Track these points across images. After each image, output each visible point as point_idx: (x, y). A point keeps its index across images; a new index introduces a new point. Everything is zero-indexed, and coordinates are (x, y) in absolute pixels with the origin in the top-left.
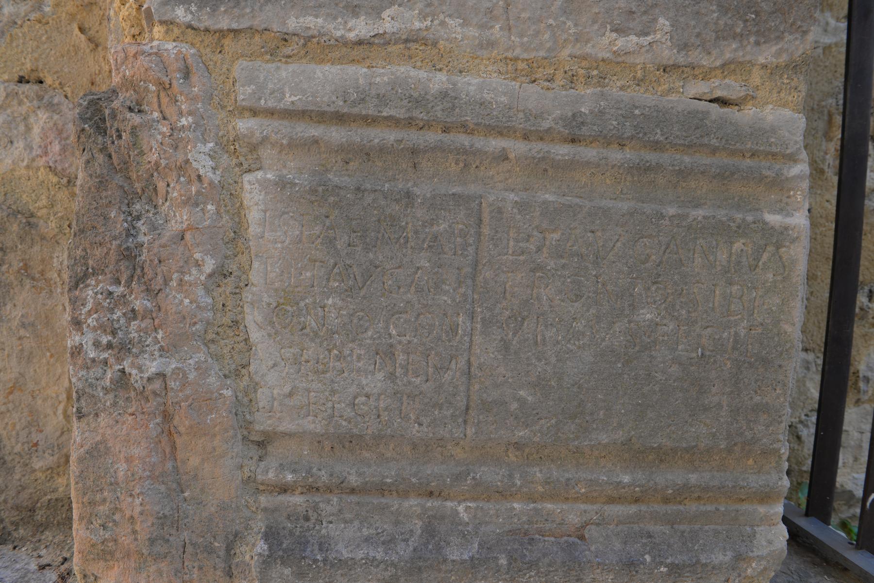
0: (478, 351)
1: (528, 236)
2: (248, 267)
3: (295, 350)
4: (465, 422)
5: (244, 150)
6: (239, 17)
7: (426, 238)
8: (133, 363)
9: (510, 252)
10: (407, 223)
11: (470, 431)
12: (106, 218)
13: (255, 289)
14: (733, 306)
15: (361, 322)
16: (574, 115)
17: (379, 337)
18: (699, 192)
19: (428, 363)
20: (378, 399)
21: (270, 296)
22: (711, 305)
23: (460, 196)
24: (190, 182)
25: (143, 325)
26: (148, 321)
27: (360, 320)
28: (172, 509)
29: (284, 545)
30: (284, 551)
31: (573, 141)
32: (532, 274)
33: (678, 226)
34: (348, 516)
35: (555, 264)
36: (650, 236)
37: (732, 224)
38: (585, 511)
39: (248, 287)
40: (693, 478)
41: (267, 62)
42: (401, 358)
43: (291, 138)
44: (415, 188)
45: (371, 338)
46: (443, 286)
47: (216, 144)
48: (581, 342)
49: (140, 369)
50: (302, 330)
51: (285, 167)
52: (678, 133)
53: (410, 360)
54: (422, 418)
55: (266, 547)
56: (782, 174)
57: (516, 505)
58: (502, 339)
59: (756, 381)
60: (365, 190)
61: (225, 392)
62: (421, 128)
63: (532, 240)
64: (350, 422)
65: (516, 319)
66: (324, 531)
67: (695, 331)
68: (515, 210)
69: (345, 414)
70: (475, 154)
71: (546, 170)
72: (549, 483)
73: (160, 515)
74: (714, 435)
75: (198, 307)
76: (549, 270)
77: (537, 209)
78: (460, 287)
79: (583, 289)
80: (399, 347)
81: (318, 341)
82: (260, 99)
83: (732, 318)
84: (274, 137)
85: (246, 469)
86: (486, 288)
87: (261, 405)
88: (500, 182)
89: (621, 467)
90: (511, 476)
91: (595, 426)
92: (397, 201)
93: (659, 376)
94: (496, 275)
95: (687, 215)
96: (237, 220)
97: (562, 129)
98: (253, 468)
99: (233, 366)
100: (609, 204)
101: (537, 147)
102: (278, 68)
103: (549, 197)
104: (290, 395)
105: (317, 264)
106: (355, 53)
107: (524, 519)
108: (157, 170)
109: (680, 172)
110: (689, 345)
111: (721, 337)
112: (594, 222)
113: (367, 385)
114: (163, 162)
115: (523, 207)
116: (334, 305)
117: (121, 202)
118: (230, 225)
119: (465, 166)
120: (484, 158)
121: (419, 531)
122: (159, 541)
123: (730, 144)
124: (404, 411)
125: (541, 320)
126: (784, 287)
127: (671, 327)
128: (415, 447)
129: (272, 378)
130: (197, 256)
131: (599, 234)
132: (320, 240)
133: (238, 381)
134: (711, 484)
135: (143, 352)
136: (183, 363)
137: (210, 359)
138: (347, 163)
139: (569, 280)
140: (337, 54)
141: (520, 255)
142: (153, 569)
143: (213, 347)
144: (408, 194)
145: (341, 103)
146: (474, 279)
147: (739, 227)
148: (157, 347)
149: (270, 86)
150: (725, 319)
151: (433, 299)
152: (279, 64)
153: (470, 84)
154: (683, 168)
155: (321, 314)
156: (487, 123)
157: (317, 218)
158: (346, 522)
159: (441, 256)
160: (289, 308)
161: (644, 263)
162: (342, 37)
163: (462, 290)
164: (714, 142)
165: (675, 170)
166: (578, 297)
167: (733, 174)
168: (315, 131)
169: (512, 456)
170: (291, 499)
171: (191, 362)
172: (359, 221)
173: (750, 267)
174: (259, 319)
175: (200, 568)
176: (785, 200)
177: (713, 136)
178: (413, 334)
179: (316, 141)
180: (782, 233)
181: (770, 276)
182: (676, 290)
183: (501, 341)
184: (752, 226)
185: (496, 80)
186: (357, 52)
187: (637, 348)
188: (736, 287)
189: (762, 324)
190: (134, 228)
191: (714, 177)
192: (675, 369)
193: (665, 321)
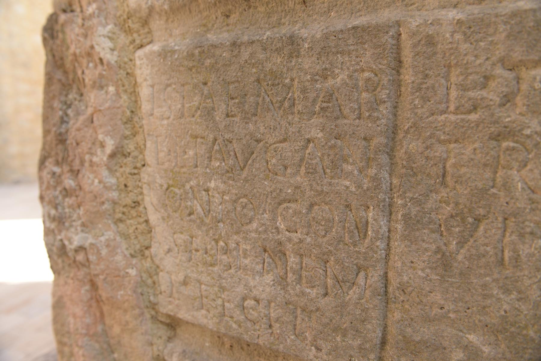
0: (399, 264)
2: (143, 147)
7: (318, 96)
9: (452, 108)
10: (292, 80)
13: (149, 169)
15: (245, 211)
17: (265, 231)
19: (326, 271)
20: (268, 306)
21: (161, 177)
24: (96, 66)
27: (244, 207)
32: (494, 143)
39: (144, 168)
42: (293, 260)
44: (303, 31)
45: (256, 231)
46: (345, 166)
47: (115, 25)
49: (69, 240)
50: (190, 214)
51: (171, 35)
53: (304, 265)
58: (438, 250)
60: (242, 43)
61: (130, 271)
63: (492, 84)
64: (240, 326)
65: (463, 219)
68: (458, 36)
69: (235, 315)
75: (105, 187)
76: (528, 137)
77: (501, 27)
80: (289, 246)
81: (204, 228)
85: (155, 348)
86: (412, 168)
87: (163, 288)
92: (278, 51)
94: (427, 148)
96: (133, 99)
98: (161, 348)
99: (138, 247)
104: (185, 283)
105: (199, 140)
108: (76, 60)
113: (255, 287)
114: (78, 51)
116: (216, 189)
117: (61, 94)
118: (127, 104)
124: (298, 327)
125: (511, 223)
129: (168, 263)
130: (100, 137)
132: (199, 112)
133: (143, 261)
135: (71, 226)
136: (96, 239)
137: (118, 238)
138: (228, 16)
141: (469, 112)
143: (121, 226)
148: (79, 222)
151: (330, 184)
155: (205, 198)
157: (195, 86)
159: (339, 122)
160: (176, 190)
163: (372, 172)
171: (102, 239)
172: (236, 84)
174: (155, 201)
178: (305, 231)
183: (436, 252)
190: (67, 115)
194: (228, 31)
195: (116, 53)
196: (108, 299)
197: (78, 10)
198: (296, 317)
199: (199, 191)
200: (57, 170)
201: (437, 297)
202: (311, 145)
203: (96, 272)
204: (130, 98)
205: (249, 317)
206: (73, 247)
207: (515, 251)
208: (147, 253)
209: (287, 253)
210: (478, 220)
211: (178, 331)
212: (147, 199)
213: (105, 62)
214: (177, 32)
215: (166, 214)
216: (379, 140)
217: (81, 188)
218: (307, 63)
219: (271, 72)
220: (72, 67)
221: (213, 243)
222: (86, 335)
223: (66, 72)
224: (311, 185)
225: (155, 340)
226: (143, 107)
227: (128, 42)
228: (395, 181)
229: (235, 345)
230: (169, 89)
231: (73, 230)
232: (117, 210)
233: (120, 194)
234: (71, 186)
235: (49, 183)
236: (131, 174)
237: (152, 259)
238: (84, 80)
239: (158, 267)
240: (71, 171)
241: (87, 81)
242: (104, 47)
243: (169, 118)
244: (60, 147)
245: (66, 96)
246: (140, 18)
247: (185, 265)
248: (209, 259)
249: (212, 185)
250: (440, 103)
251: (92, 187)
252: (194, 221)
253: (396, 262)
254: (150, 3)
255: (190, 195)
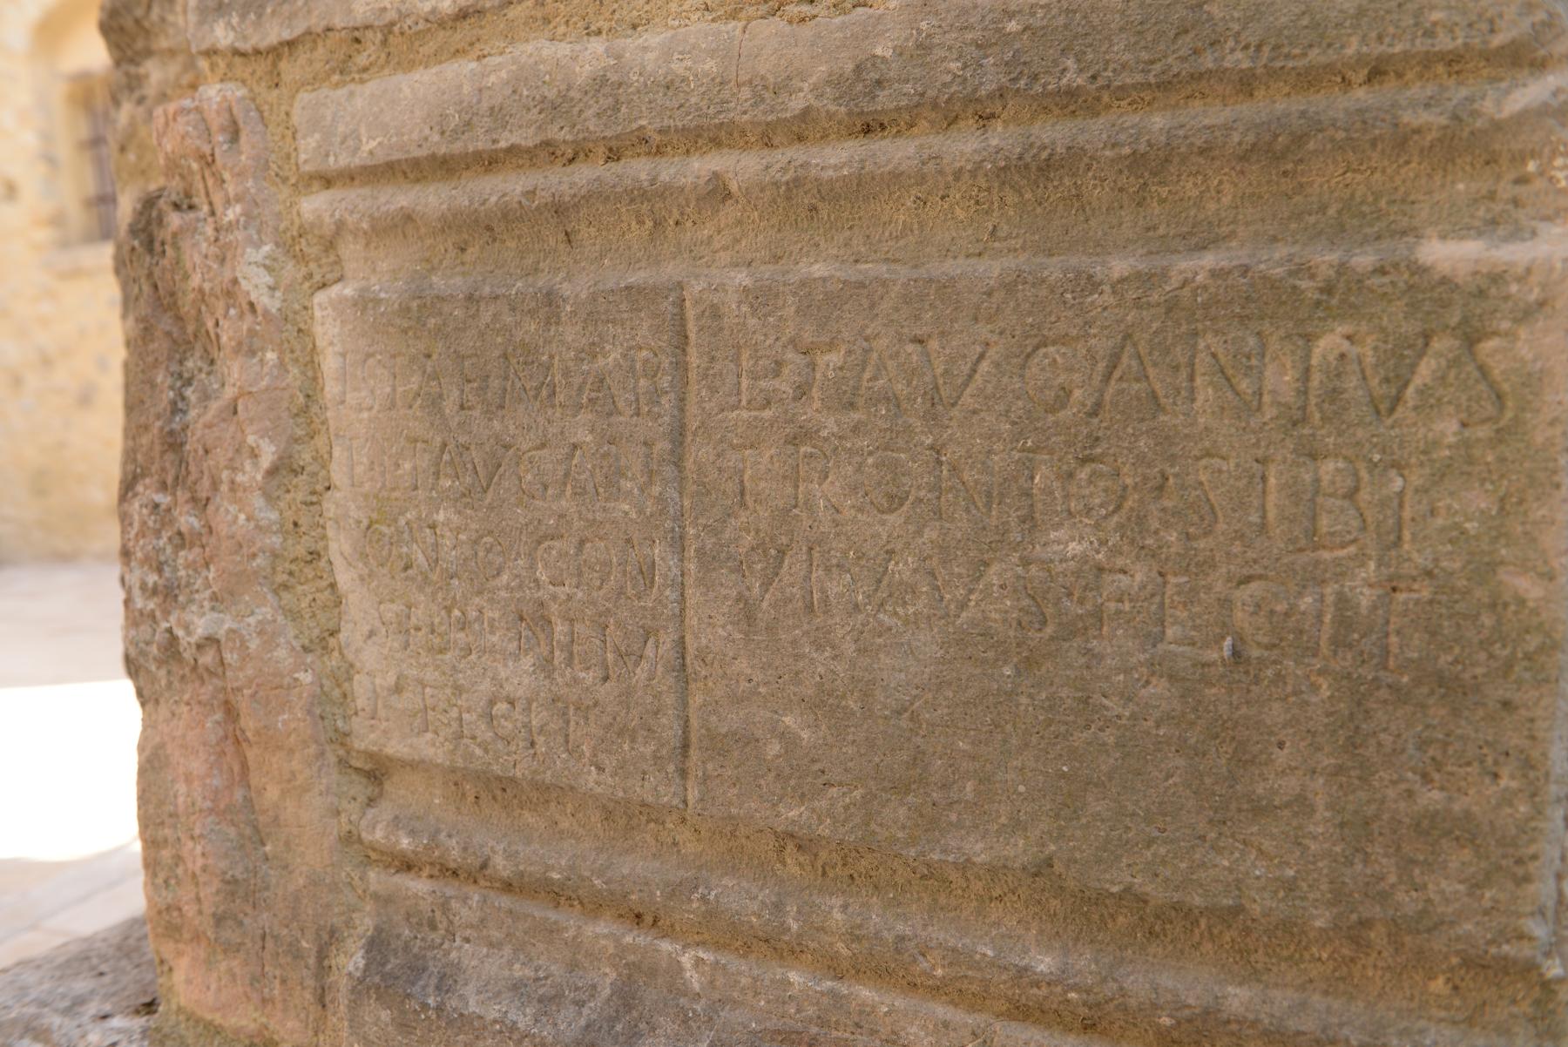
0: (695, 622)
1: (776, 362)
3: (397, 607)
4: (683, 773)
5: (313, 251)
6: (289, 18)
7: (584, 383)
8: (179, 619)
9: (744, 403)
10: (551, 357)
11: (693, 795)
12: (153, 385)
13: (338, 495)
14: (1324, 523)
15: (490, 556)
16: (858, 69)
17: (520, 586)
18: (1212, 206)
19: (604, 642)
21: (359, 508)
22: (1254, 518)
23: (641, 290)
24: (241, 316)
25: (191, 557)
26: (197, 550)
27: (488, 551)
28: (246, 869)
29: (389, 967)
30: (384, 977)
31: (867, 130)
33: (1137, 304)
34: (496, 935)
35: (838, 423)
36: (1063, 340)
37: (1304, 284)
38: (946, 1025)
40: (1238, 998)
41: (337, 86)
42: (560, 628)
43: (371, 216)
44: (565, 285)
45: (507, 587)
46: (622, 482)
47: (277, 245)
48: (911, 610)
49: (187, 628)
50: (406, 568)
52: (1127, 57)
54: (602, 756)
55: (362, 963)
56: (1475, 114)
57: (794, 976)
59: (1423, 744)
61: (301, 676)
62: (571, 161)
63: (786, 371)
64: (486, 751)
66: (454, 955)
67: (1209, 588)
68: (745, 308)
70: (662, 196)
71: (813, 208)
72: (858, 939)
73: (228, 877)
74: (1291, 886)
75: (258, 527)
76: (826, 439)
77: (790, 300)
78: (650, 482)
79: (904, 480)
80: (554, 607)
81: (429, 590)
82: (327, 155)
83: (1326, 555)
84: (351, 220)
85: (344, 819)
87: (360, 703)
88: (725, 248)
89: (1041, 932)
90: (778, 907)
91: (954, 817)
92: (532, 313)
93: (1113, 705)
94: (718, 456)
95: (1164, 275)
96: (310, 374)
97: (833, 108)
99: (316, 632)
100: (953, 267)
101: (788, 156)
102: (352, 94)
103: (819, 270)
104: (398, 689)
106: (458, 36)
107: (811, 1011)
108: (203, 300)
109: (1136, 161)
110: (1194, 628)
111: (1293, 607)
112: (917, 318)
114: (207, 286)
115: (760, 298)
117: (170, 358)
118: (298, 383)
119: (657, 224)
120: (682, 201)
121: (608, 991)
122: (230, 922)
123: (1287, 56)
124: (571, 738)
125: (816, 555)
126: (1502, 460)
127: (1139, 577)
128: (608, 815)
129: (369, 657)
130: (251, 439)
131: (934, 344)
132: (419, 401)
133: (325, 658)
134: (1292, 1024)
135: (191, 601)
137: (280, 618)
138: (463, 250)
139: (870, 461)
140: (430, 47)
142: (223, 966)
143: (286, 596)
144: (550, 299)
145: (436, 138)
146: (678, 464)
147: (1328, 290)
148: (207, 593)
149: (341, 129)
150: (1304, 558)
152: (352, 86)
153: (647, 51)
154: (1143, 148)
155: (430, 540)
156: (680, 124)
157: (413, 359)
158: (491, 945)
159: (612, 419)
160: (384, 529)
161: (1052, 410)
162: (434, 11)
163: (656, 490)
164: (1238, 60)
165: (1120, 158)
166: (895, 501)
167: (1299, 139)
168: (399, 198)
169: (793, 864)
170: (411, 884)
171: (251, 620)
172: (474, 360)
173: (1374, 403)
174: (347, 548)
175: (284, 981)
176: (1506, 190)
177: (1231, 43)
178: (574, 581)
179: (408, 217)
180: (1481, 293)
181: (1448, 428)
182: (1145, 478)
184: (1376, 281)
185: (700, 30)
186: (459, 37)
187: (1049, 630)
188: (1328, 467)
189: (1429, 574)
190: (183, 398)
191: (1243, 158)
192: (1159, 687)
193: (1120, 562)
194: (463, 274)
195: (278, 294)
196: (257, 733)
197: (206, 208)
198: (568, 722)
199: (421, 528)
200: (163, 499)
201: (742, 665)
202: (578, 453)
203: (235, 685)
204: (303, 373)
205: (500, 732)
206: (193, 640)
207: (823, 591)
208: (332, 642)
209: (553, 619)
210: (782, 553)
211: (387, 786)
212: (333, 546)
213: (259, 309)
214: (383, 266)
215: (367, 571)
216: (662, 446)
217: (211, 532)
218: (570, 332)
219: (523, 344)
220: (193, 312)
221: (443, 613)
222: (211, 811)
223: (179, 318)
224: (580, 513)
225: (344, 804)
226: (327, 389)
227: (299, 276)
228: (686, 503)
229: (483, 795)
230: (371, 361)
231: (194, 608)
232: (279, 569)
233: (285, 540)
234: (192, 528)
235: (144, 523)
236: (305, 503)
237: (341, 653)
238: (218, 336)
239: (352, 666)
240: (194, 499)
241: (224, 339)
242: (256, 283)
243: (371, 409)
244: (170, 456)
245: (181, 362)
246: (321, 237)
247: (398, 655)
248: (437, 641)
249: (441, 517)
250: (730, 395)
251: (234, 528)
252: (413, 579)
253: (692, 620)
254: (337, 215)
255: (406, 536)
